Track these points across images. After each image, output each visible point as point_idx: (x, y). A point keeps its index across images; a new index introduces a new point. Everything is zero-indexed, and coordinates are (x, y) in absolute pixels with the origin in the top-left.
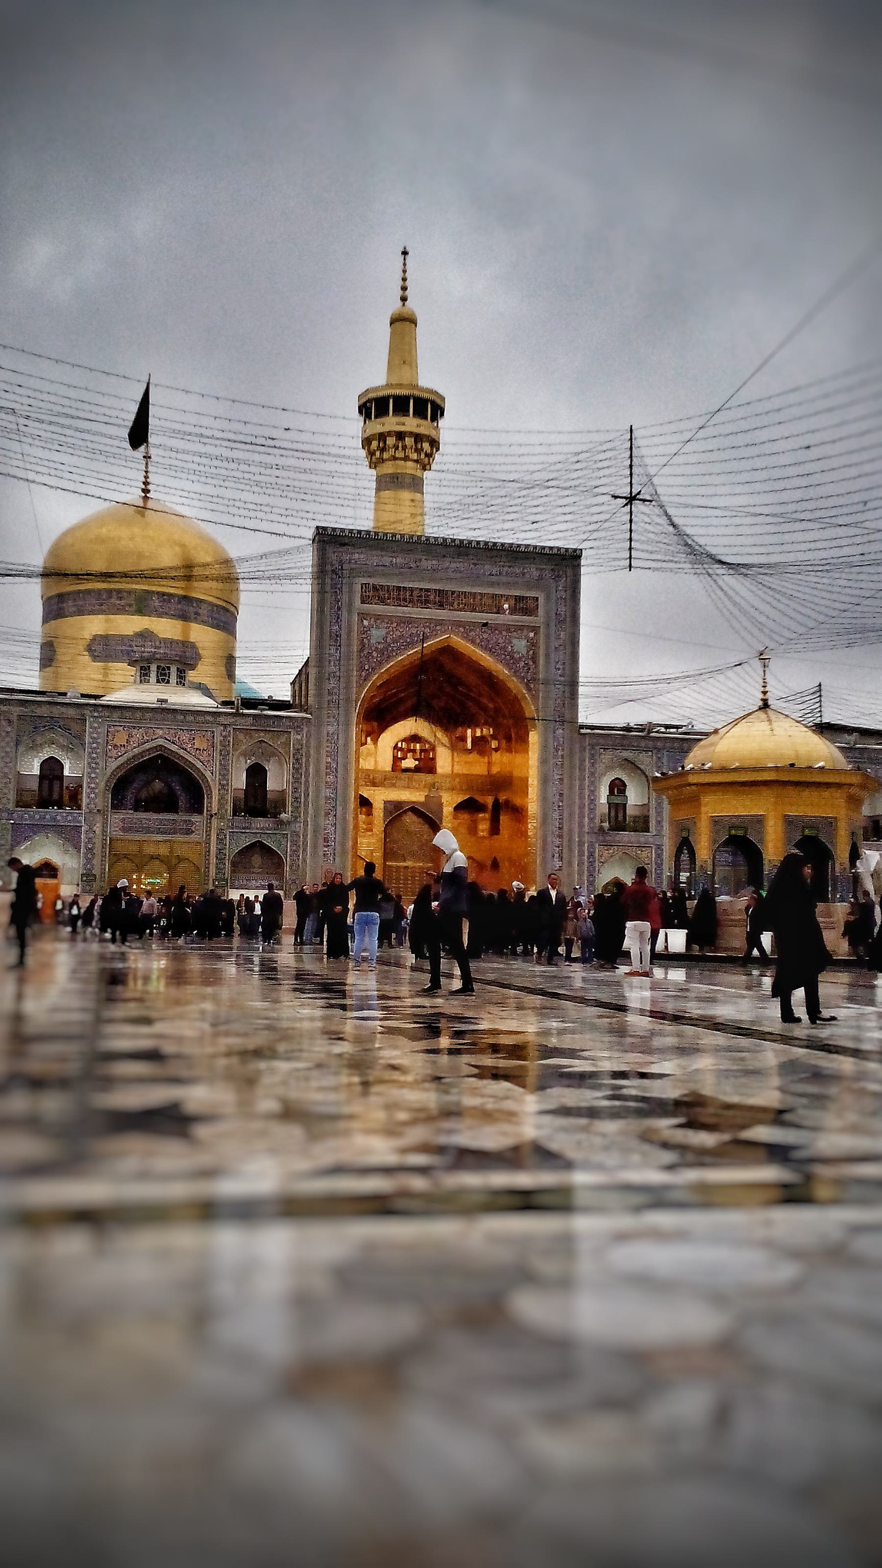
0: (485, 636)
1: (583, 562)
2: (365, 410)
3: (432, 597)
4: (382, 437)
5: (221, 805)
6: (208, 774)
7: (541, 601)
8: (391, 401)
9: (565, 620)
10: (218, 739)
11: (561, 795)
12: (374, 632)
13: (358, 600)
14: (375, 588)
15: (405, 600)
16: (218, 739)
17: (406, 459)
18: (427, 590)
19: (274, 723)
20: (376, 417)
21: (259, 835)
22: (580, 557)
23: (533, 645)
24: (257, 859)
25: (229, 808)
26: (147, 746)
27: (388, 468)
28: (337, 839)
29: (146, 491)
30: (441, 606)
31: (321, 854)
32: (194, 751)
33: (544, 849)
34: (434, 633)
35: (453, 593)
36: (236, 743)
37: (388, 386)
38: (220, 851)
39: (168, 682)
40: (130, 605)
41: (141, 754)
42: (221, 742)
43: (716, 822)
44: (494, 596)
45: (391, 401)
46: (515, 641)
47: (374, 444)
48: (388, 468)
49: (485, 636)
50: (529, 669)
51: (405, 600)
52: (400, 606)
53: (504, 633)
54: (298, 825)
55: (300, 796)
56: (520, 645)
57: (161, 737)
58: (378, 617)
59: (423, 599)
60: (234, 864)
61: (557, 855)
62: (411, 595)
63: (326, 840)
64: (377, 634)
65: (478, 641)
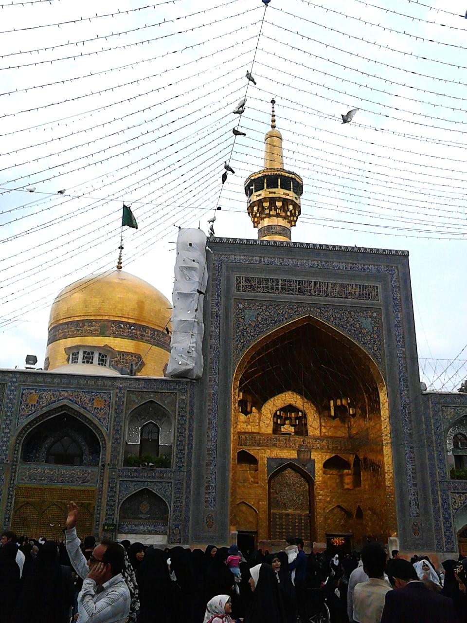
2: (248, 192)
3: (293, 286)
4: (260, 202)
5: (114, 457)
6: (104, 430)
9: (400, 302)
10: (113, 400)
14: (248, 280)
15: (272, 288)
16: (113, 401)
20: (255, 192)
22: (408, 256)
23: (376, 322)
24: (145, 506)
25: (121, 458)
26: (54, 406)
29: (119, 268)
34: (297, 313)
35: (310, 283)
36: (129, 401)
38: (111, 498)
39: (92, 363)
41: (49, 413)
44: (342, 286)
47: (255, 209)
50: (375, 341)
51: (272, 288)
52: (268, 292)
54: (182, 473)
55: (184, 449)
56: (367, 323)
57: (66, 398)
59: (287, 288)
60: (123, 509)
63: (207, 488)
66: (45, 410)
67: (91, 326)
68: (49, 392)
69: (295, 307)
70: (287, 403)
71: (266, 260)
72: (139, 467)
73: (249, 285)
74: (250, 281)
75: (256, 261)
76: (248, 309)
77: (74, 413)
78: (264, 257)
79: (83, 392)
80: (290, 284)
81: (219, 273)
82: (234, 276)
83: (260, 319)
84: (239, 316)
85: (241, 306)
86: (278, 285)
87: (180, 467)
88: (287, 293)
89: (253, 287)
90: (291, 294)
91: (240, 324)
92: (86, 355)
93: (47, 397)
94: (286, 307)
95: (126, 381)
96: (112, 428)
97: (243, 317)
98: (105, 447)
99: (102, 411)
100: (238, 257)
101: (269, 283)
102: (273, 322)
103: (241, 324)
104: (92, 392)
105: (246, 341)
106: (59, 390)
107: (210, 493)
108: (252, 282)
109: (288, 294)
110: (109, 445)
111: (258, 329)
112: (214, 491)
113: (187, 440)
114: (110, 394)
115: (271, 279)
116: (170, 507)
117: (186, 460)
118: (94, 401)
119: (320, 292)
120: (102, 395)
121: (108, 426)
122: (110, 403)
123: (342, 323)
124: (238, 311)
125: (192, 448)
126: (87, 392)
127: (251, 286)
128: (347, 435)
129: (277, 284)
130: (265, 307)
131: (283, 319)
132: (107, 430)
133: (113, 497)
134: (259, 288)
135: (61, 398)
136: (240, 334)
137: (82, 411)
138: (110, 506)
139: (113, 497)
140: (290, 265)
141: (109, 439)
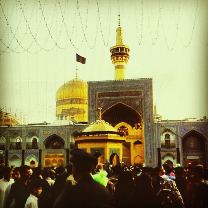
1: (153, 80)
5: (68, 146)
6: (64, 140)
7: (142, 92)
8: (120, 49)
11: (150, 139)
13: (97, 97)
14: (101, 94)
17: (123, 62)
27: (117, 64)
32: (61, 134)
33: (146, 153)
36: (70, 131)
37: (116, 46)
39: (63, 119)
40: (69, 102)
43: (110, 149)
45: (120, 49)
46: (136, 102)
47: (113, 59)
48: (117, 64)
49: (128, 102)
53: (133, 100)
56: (137, 103)
57: (55, 132)
58: (102, 100)
61: (150, 155)
65: (127, 103)
67: (68, 101)
82: (98, 92)
85: (99, 102)
110: (66, 144)
137: (59, 135)
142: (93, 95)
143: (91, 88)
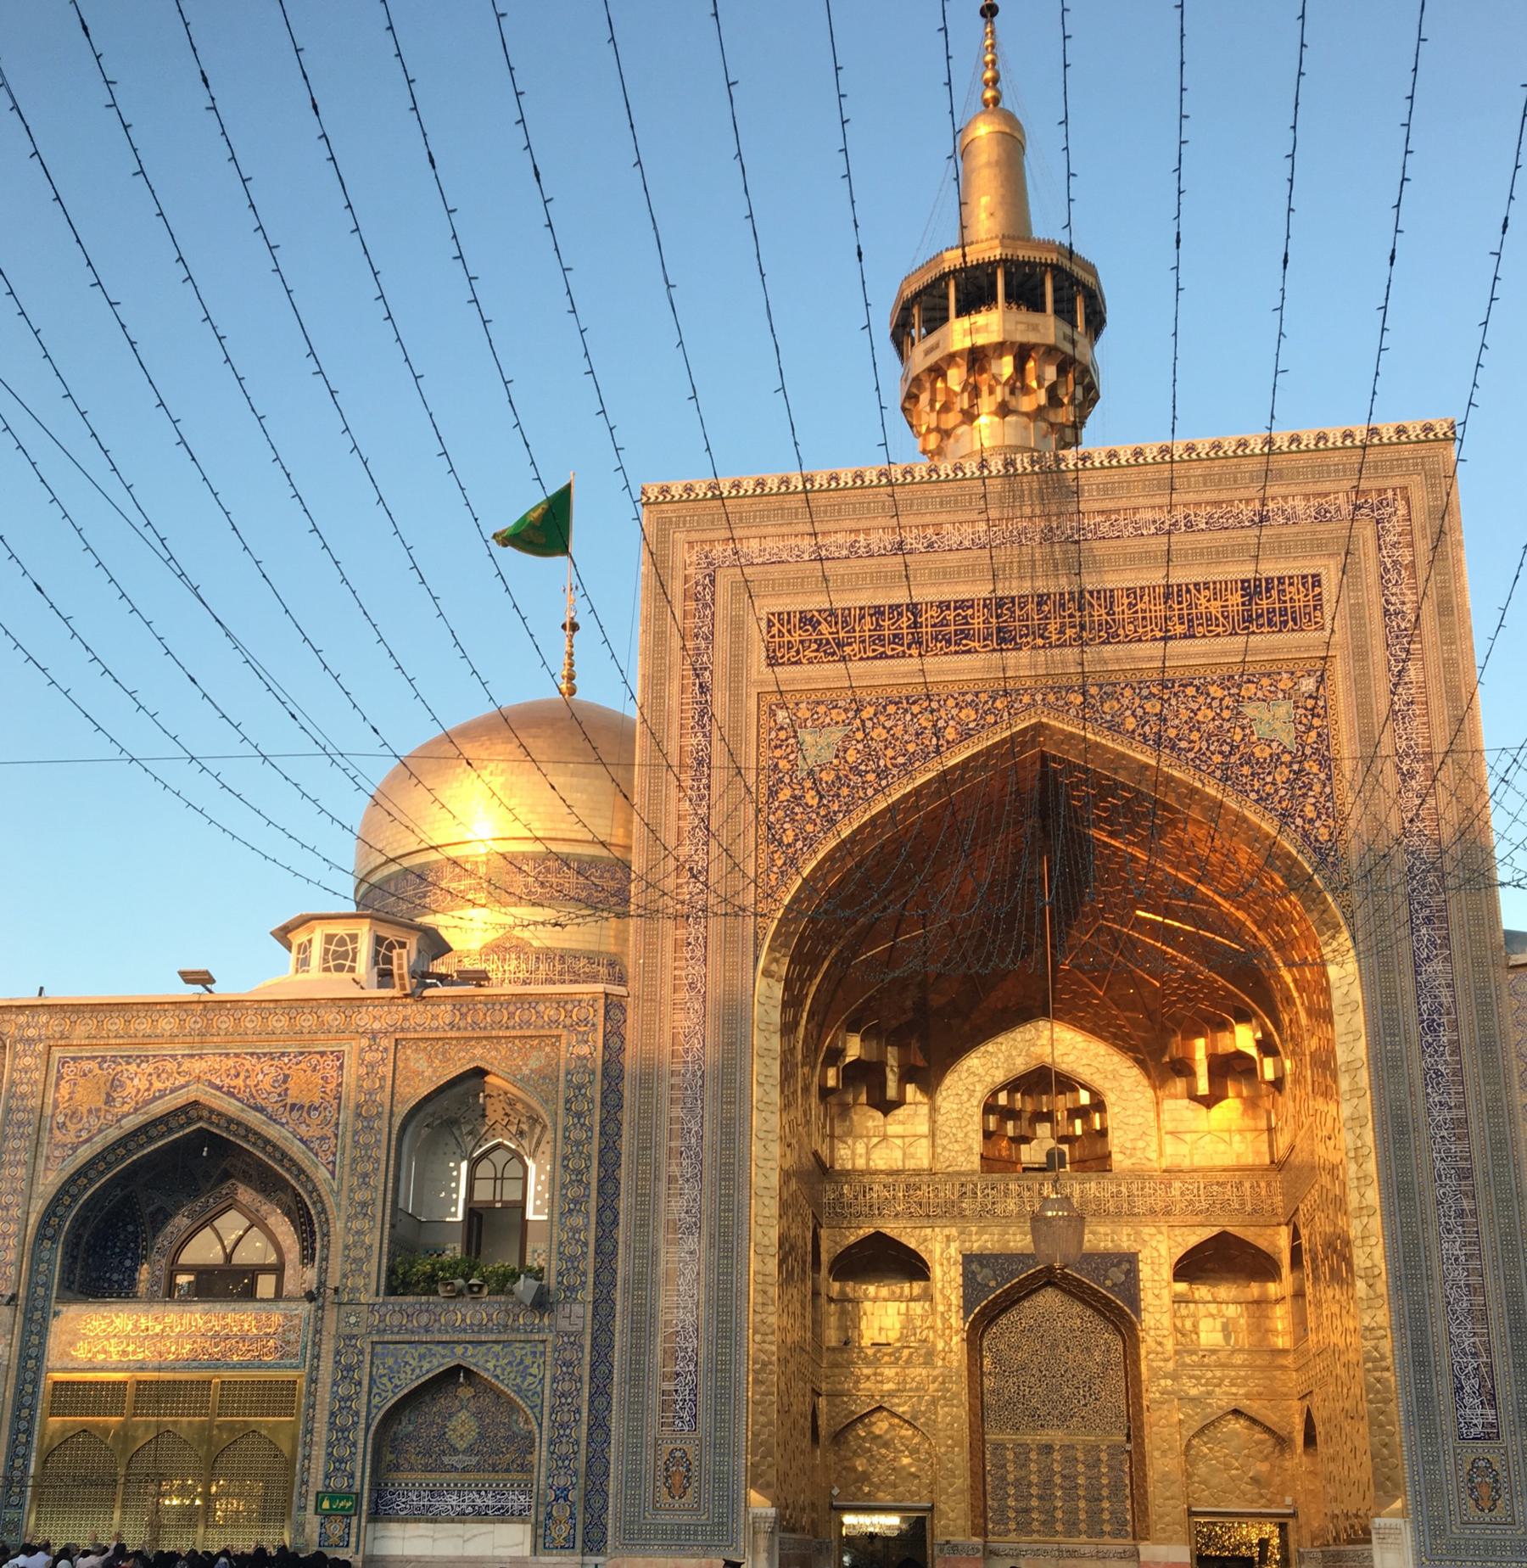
0: (1153, 707)
3: (977, 623)
12: (807, 737)
13: (758, 655)
14: (807, 620)
18: (961, 605)
19: (511, 1015)
21: (459, 1350)
28: (702, 1353)
30: (1004, 639)
31: (655, 1401)
34: (991, 719)
35: (1042, 600)
42: (360, 1078)
49: (1153, 707)
51: (897, 638)
54: (577, 1309)
62: (916, 625)
64: (819, 746)
65: (1131, 724)
66: (130, 1123)
68: (144, 1065)
69: (983, 697)
70: (1021, 1065)
71: (874, 537)
72: (436, 1293)
73: (814, 637)
74: (815, 624)
75: (839, 547)
76: (809, 723)
77: (227, 1129)
78: (867, 531)
79: (252, 1054)
80: (965, 617)
81: (706, 606)
83: (851, 756)
84: (778, 753)
86: (916, 625)
87: (571, 1288)
88: (953, 648)
89: (828, 642)
90: (969, 652)
91: (781, 780)
92: (332, 948)
93: (136, 1081)
94: (951, 702)
95: (394, 1009)
96: (347, 1169)
97: (792, 757)
98: (327, 1234)
99: (314, 1114)
100: (769, 543)
101: (886, 623)
102: (901, 760)
103: (787, 779)
104: (283, 1054)
105: (805, 839)
106: (174, 1057)
107: (678, 1375)
108: (824, 627)
109: (956, 652)
110: (337, 1226)
111: (845, 791)
112: (692, 1368)
113: (594, 1194)
114: (339, 1056)
115: (890, 607)
116: (540, 1425)
117: (589, 1264)
118: (291, 1084)
119: (1083, 627)
120: (314, 1062)
121: (334, 1163)
122: (340, 1085)
123: (1172, 733)
124: (773, 735)
125: (615, 1223)
126: (265, 1054)
127: (819, 643)
128: (1267, 1161)
129: (915, 622)
130: (871, 710)
131: (938, 746)
132: (333, 1173)
133: (350, 1398)
134: (850, 644)
135: (182, 1081)
136: (780, 813)
138: (340, 1432)
139: (350, 1398)
140: (967, 543)
141: (338, 1205)
142: (710, 638)
143: (685, 558)
